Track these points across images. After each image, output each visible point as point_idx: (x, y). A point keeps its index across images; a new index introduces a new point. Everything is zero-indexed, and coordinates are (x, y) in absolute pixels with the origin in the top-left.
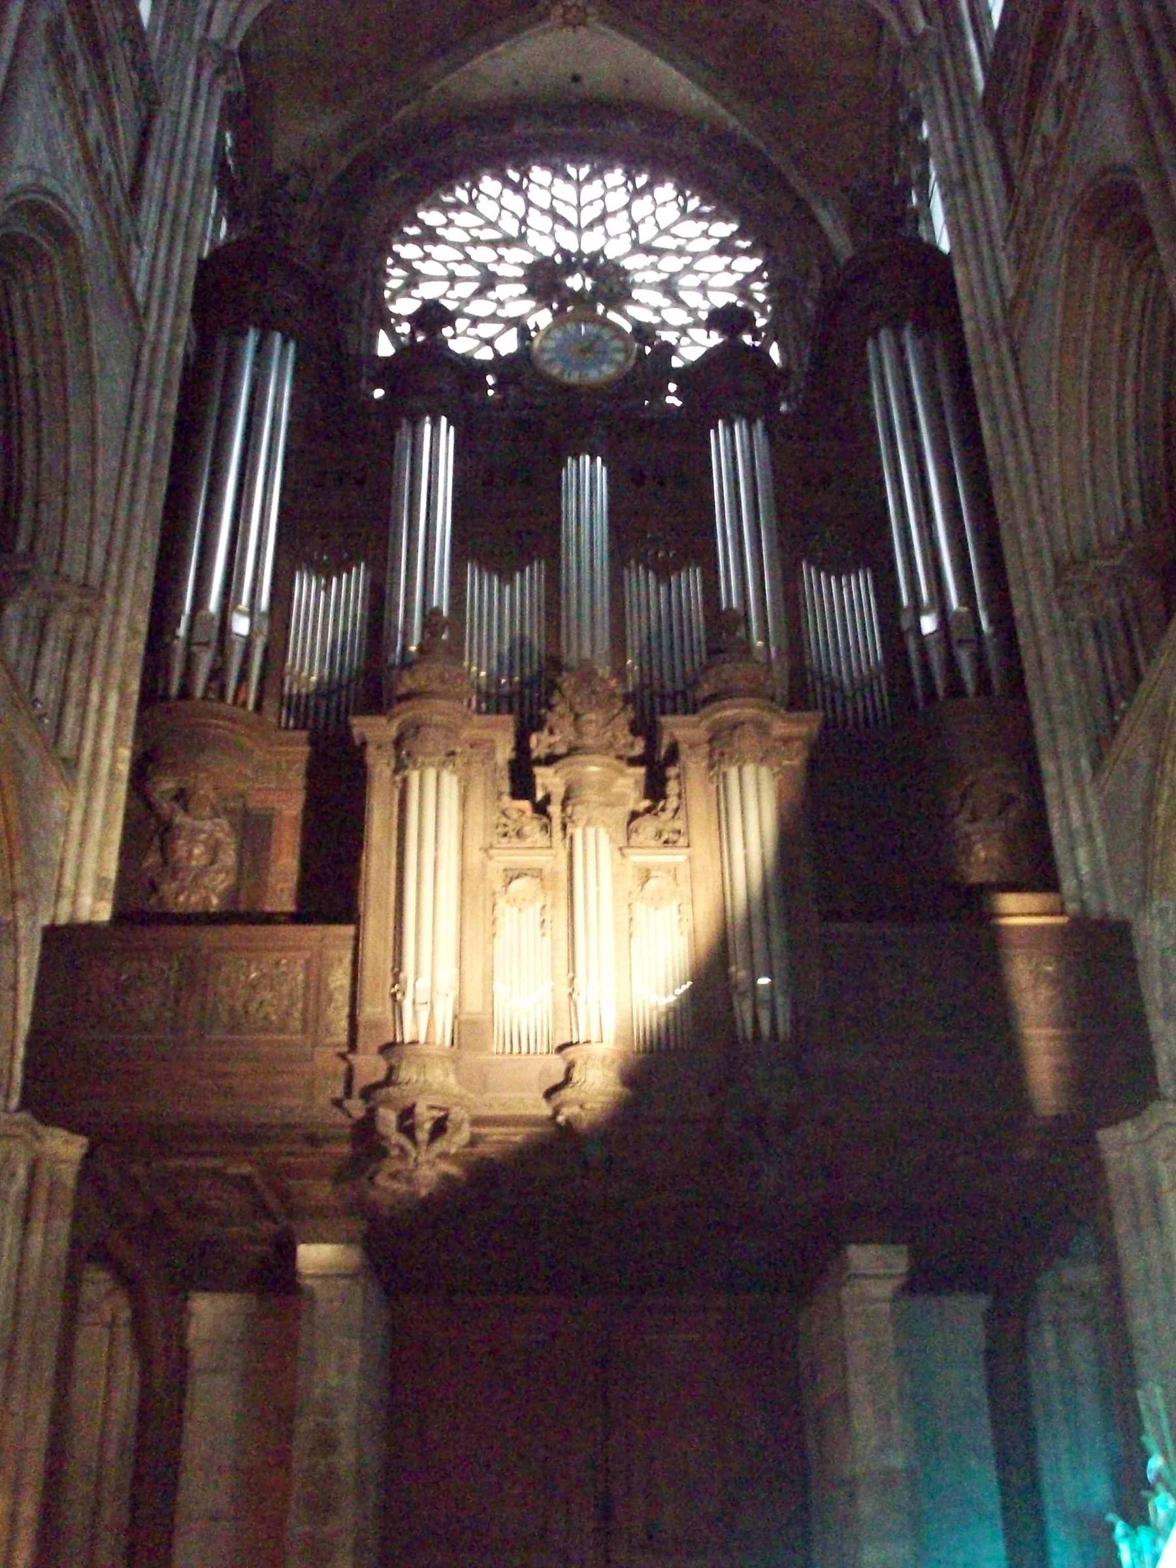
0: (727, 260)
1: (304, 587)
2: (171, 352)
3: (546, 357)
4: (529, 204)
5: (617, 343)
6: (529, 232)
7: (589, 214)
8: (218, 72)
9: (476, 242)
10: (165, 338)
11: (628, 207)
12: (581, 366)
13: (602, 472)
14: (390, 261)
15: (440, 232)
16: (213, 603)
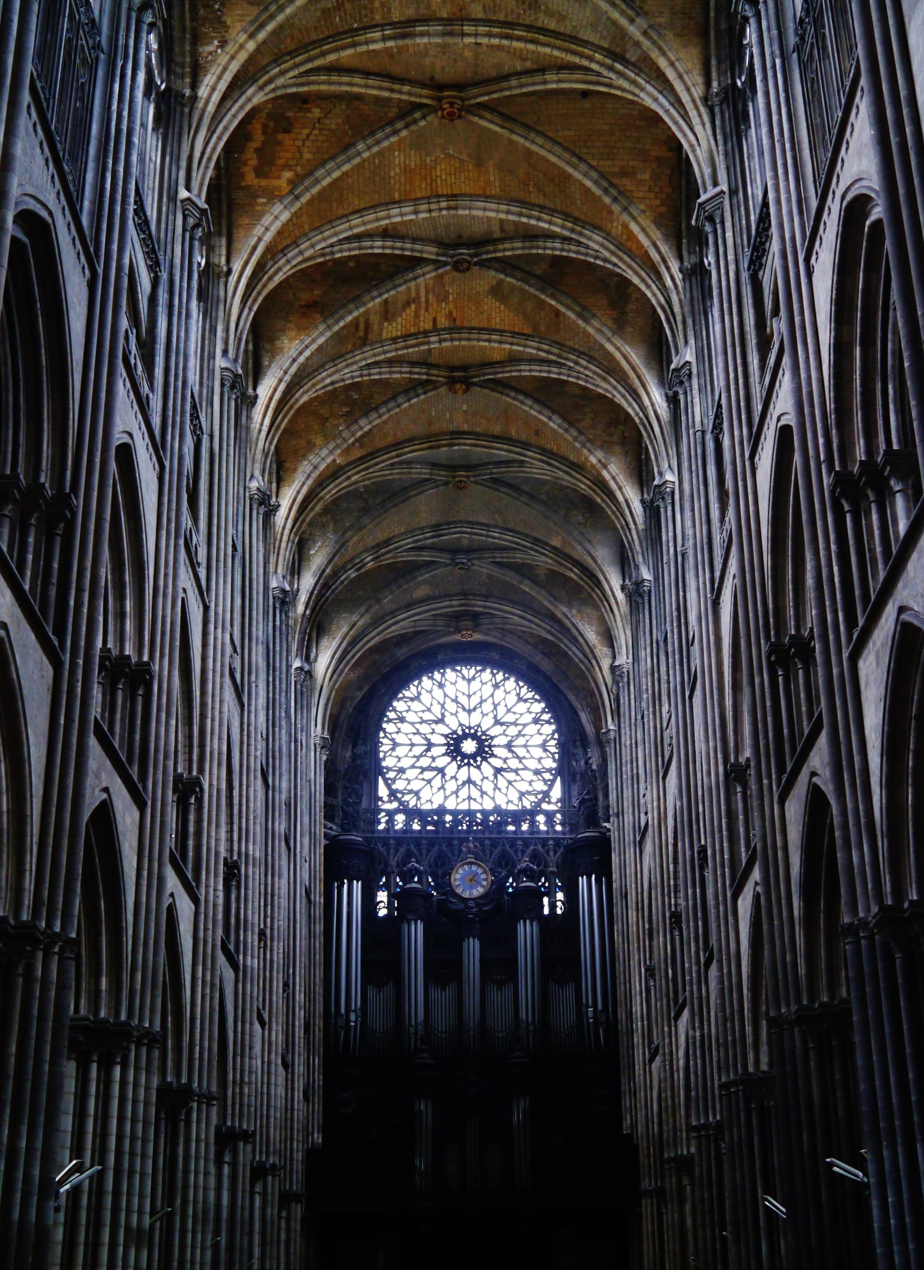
0: (538, 726)
1: (372, 992)
2: (320, 902)
3: (457, 883)
4: (446, 695)
5: (484, 876)
6: (446, 713)
7: (475, 700)
8: (322, 748)
9: (423, 721)
10: (318, 900)
11: (492, 695)
12: (471, 888)
13: (477, 943)
14: (382, 734)
15: (404, 714)
16: (343, 1011)
